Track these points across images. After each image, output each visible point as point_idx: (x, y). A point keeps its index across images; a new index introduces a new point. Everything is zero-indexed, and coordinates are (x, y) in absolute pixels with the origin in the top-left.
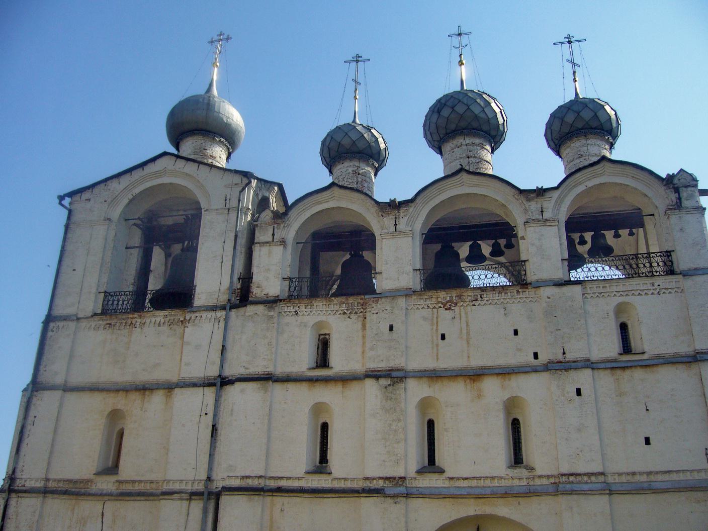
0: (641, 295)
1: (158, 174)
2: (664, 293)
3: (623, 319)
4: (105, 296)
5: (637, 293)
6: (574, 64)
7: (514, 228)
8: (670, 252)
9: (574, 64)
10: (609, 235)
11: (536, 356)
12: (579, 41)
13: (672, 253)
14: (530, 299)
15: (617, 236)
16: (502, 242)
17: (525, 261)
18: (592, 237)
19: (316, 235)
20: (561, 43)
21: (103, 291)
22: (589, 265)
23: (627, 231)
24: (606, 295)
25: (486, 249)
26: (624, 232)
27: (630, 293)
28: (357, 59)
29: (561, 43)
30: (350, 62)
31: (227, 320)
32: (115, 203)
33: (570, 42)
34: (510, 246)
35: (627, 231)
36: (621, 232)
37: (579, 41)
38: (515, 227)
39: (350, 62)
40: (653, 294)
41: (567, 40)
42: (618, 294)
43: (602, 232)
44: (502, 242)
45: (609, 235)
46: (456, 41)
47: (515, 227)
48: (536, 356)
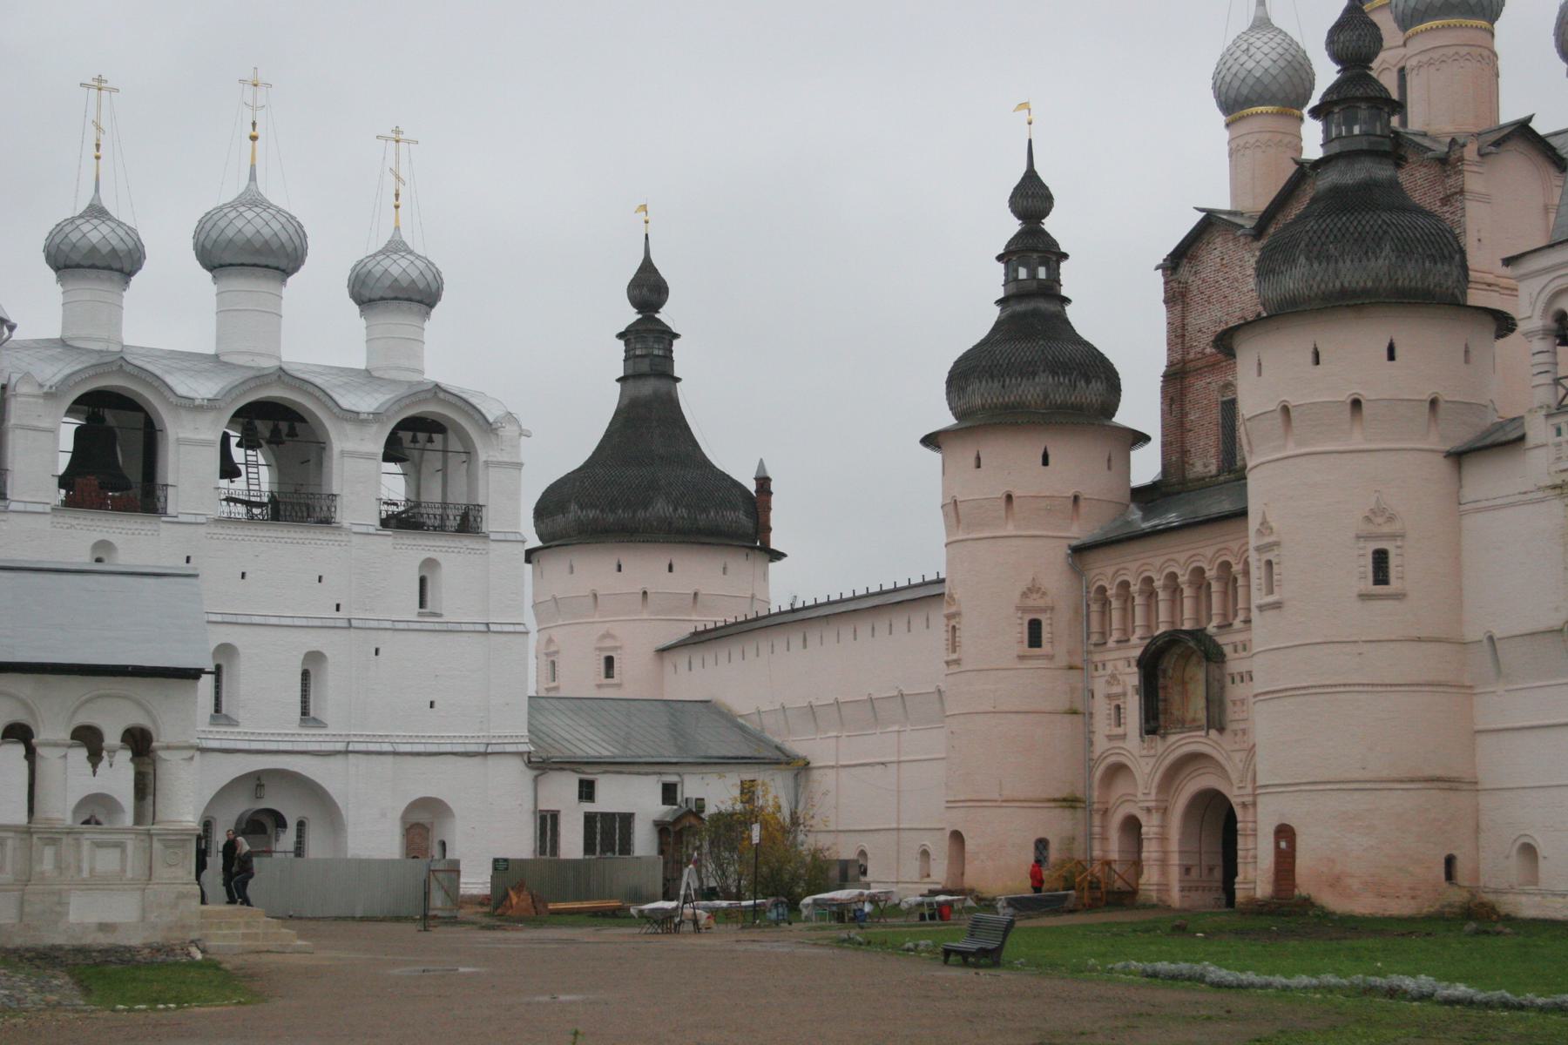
2: (470, 553)
3: (424, 574)
5: (444, 549)
6: (398, 177)
8: (481, 506)
9: (398, 177)
10: (406, 436)
11: (338, 607)
12: (409, 142)
13: (483, 508)
17: (335, 495)
20: (387, 139)
26: (421, 436)
28: (99, 84)
29: (387, 139)
30: (88, 86)
33: (397, 141)
34: (292, 433)
37: (409, 142)
39: (88, 86)
41: (394, 135)
44: (284, 426)
46: (249, 90)
48: (338, 607)
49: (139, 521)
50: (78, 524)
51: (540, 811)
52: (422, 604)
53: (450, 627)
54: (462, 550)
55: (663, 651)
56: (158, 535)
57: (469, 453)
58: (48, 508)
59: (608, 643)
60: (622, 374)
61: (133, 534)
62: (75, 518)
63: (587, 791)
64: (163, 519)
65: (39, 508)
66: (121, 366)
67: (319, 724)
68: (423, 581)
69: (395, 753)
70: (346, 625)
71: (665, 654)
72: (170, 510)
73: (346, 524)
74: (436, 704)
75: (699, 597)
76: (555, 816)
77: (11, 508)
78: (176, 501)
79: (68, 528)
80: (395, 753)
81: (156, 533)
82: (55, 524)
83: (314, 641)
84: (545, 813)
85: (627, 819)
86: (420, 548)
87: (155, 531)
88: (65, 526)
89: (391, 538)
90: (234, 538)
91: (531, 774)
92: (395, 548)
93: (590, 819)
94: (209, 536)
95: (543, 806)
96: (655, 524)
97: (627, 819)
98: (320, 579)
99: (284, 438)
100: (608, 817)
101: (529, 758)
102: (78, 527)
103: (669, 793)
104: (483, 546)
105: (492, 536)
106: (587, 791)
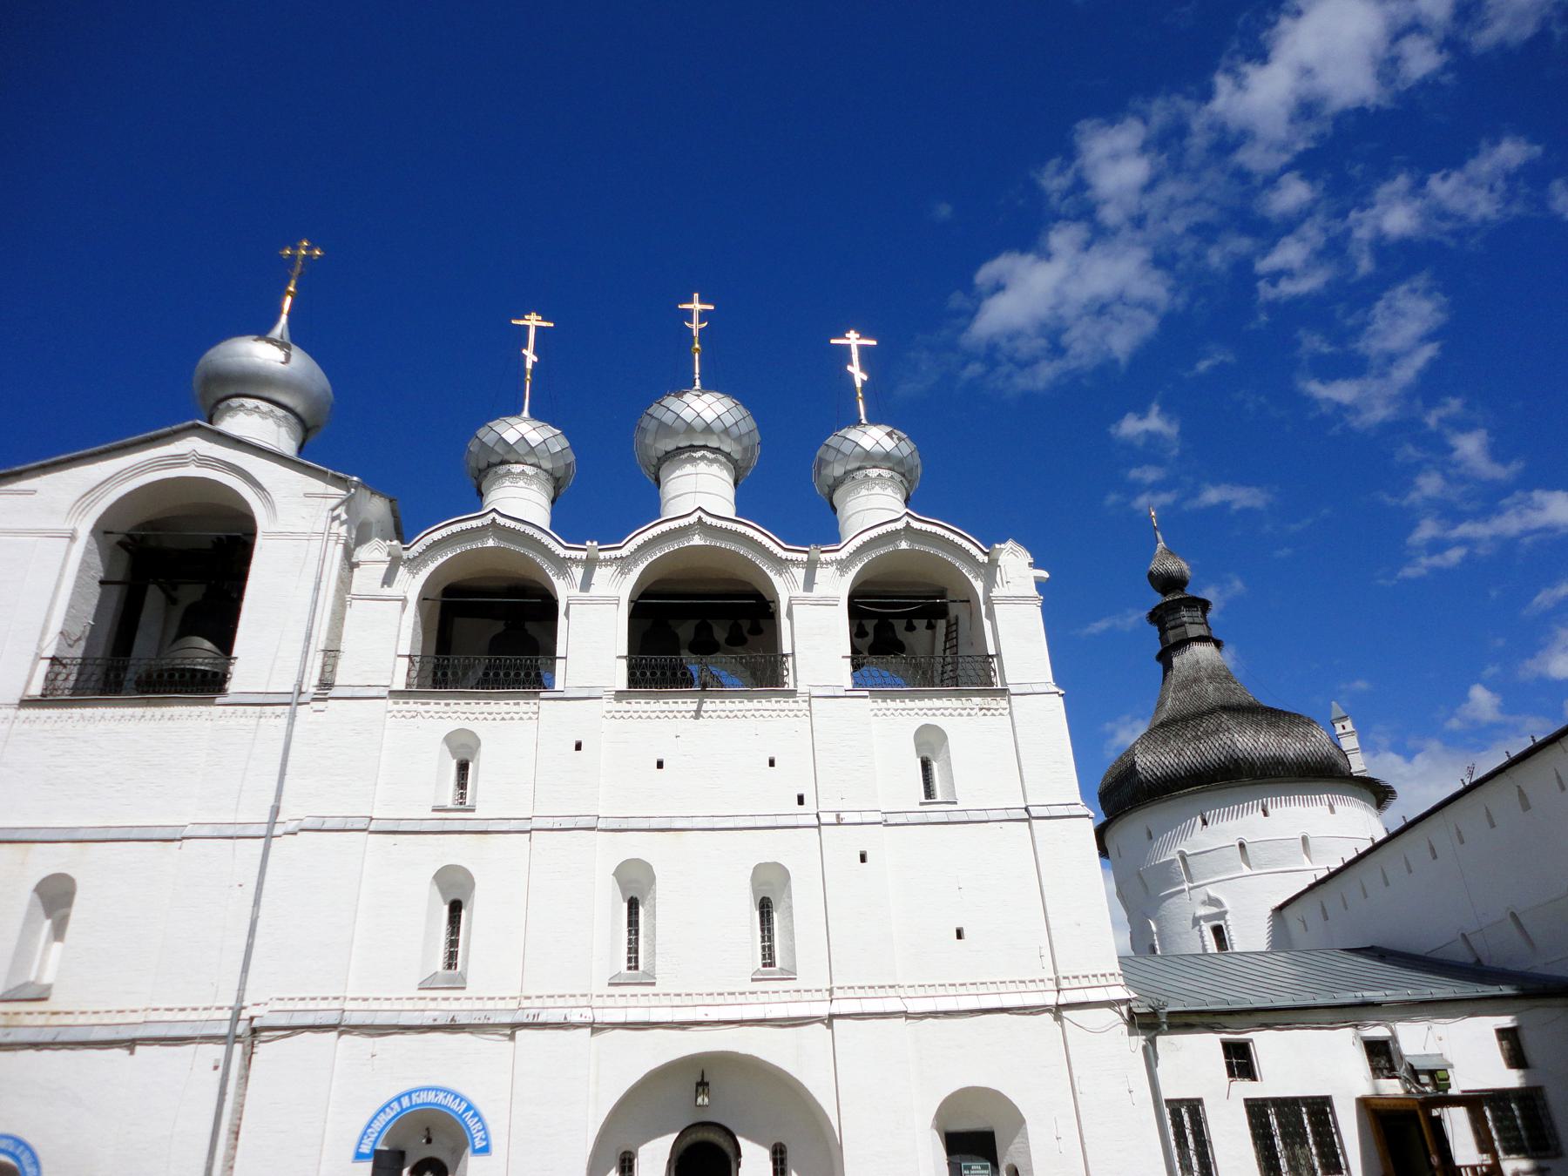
0: (953, 716)
1: (180, 460)
2: (985, 715)
4: (52, 665)
7: (771, 604)
11: (801, 800)
14: (795, 712)
15: (910, 628)
16: (746, 624)
18: (876, 628)
19: (449, 591)
21: (51, 656)
22: (873, 669)
23: (925, 622)
24: (904, 713)
25: (720, 633)
31: (293, 716)
32: (87, 502)
35: (925, 622)
36: (916, 622)
38: (773, 602)
40: (969, 715)
43: (890, 620)
44: (746, 624)
45: (900, 625)
47: (773, 602)
48: (801, 800)
49: (511, 702)
50: (428, 712)
51: (1167, 1101)
52: (929, 792)
54: (973, 712)
55: (1281, 908)
56: (538, 718)
57: (968, 601)
58: (385, 694)
59: (1214, 910)
60: (1159, 648)
61: (503, 719)
62: (423, 704)
63: (1240, 1061)
64: (542, 695)
66: (494, 520)
67: (789, 975)
69: (906, 1015)
70: (816, 823)
71: (1285, 912)
72: (559, 685)
74: (966, 933)
75: (1311, 841)
76: (1195, 1106)
78: (566, 674)
79: (413, 717)
80: (906, 1015)
83: (768, 848)
84: (1177, 1105)
85: (1320, 1108)
86: (912, 713)
87: (534, 713)
88: (408, 715)
89: (868, 700)
90: (646, 715)
91: (1140, 1040)
92: (876, 715)
93: (1256, 1109)
95: (1168, 1093)
96: (1231, 766)
97: (1320, 1108)
98: (772, 763)
99: (746, 634)
100: (1288, 1106)
101: (1130, 1010)
103: (1381, 1055)
104: (1004, 703)
105: (1013, 689)
106: (1240, 1061)
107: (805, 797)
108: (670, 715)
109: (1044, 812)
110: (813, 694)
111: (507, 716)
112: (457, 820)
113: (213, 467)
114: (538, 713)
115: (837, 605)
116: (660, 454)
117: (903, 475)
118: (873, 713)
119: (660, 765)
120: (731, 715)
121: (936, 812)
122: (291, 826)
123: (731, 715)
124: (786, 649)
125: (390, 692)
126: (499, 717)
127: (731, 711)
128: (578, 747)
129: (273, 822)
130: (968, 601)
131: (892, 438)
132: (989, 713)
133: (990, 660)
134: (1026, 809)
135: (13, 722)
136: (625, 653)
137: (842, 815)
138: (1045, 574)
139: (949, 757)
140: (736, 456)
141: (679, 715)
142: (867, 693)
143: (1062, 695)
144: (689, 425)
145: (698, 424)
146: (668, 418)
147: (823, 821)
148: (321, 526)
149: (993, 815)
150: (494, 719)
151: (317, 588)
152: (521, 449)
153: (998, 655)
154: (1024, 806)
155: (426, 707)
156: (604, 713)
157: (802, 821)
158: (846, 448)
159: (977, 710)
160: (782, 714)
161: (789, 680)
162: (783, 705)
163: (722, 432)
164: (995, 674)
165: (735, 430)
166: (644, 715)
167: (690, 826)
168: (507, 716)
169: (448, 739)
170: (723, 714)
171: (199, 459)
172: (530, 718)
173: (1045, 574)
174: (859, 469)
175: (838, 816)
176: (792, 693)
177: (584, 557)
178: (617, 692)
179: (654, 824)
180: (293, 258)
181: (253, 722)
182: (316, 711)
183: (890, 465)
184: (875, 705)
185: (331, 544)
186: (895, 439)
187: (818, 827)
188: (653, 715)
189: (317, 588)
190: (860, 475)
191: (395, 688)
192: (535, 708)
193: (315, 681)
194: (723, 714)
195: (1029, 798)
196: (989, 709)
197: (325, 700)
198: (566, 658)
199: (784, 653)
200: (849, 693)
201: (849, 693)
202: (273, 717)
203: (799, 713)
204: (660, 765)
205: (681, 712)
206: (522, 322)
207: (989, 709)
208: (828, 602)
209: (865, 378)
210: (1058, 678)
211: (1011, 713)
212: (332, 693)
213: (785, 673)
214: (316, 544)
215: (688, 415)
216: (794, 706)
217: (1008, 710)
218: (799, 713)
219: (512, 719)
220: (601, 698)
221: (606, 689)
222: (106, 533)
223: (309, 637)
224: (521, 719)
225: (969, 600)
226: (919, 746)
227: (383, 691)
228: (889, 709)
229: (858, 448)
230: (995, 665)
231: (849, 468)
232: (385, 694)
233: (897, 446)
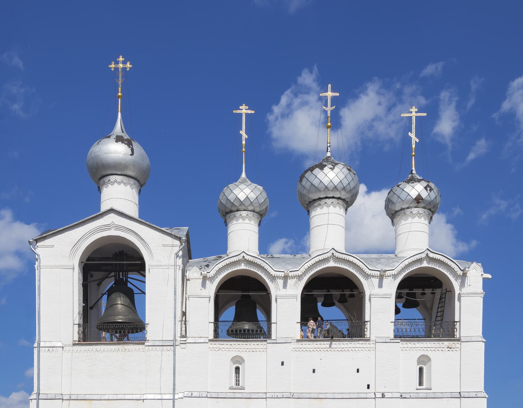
2: (449, 350)
5: (432, 349)
24: (414, 349)
27: (429, 349)
31: (174, 351)
38: (362, 293)
42: (421, 349)
47: (362, 293)
53: (437, 395)
54: (443, 349)
57: (451, 291)
64: (268, 341)
65: (202, 340)
68: (421, 370)
70: (374, 397)
73: (372, 338)
77: (188, 341)
81: (265, 350)
82: (211, 349)
88: (217, 349)
92: (402, 350)
94: (294, 350)
102: (223, 350)
107: (370, 385)
108: (318, 350)
109: (467, 395)
110: (377, 341)
111: (254, 350)
112: (238, 393)
113: (122, 230)
114: (267, 349)
115: (391, 298)
116: (310, 200)
117: (430, 210)
118: (401, 349)
119: (314, 371)
120: (343, 350)
121: (423, 393)
122: (181, 395)
123: (343, 350)
124: (367, 318)
125: (209, 340)
126: (251, 350)
127: (343, 348)
128: (283, 364)
129: (174, 394)
130: (451, 291)
131: (427, 190)
132: (450, 350)
133: (456, 323)
134: (460, 393)
135: (72, 352)
136: (300, 321)
137: (385, 394)
138: (489, 276)
139: (431, 369)
140: (347, 200)
141: (322, 350)
142: (399, 341)
143: (485, 342)
144: (326, 187)
145: (331, 186)
146: (316, 182)
147: (377, 396)
148: (172, 262)
149: (445, 395)
150: (249, 351)
151: (175, 294)
152: (247, 203)
153: (459, 322)
154: (459, 392)
155: (223, 346)
156: (292, 349)
157: (369, 396)
158: (403, 196)
159: (446, 348)
160: (363, 349)
161: (367, 334)
162: (365, 346)
163: (342, 190)
164: (457, 331)
165: (348, 188)
166: (308, 350)
167: (325, 397)
168: (254, 350)
169: (232, 359)
170: (339, 349)
171: (115, 227)
172: (263, 351)
173: (489, 276)
174: (408, 208)
175: (383, 394)
176: (368, 340)
177: (283, 276)
178: (297, 340)
179: (312, 396)
180: (116, 69)
181: (160, 353)
182: (182, 348)
183: (424, 205)
184: (402, 346)
185: (177, 270)
186: (428, 191)
187: (375, 398)
188: (311, 350)
189: (175, 294)
190: (408, 211)
191: (210, 339)
192: (265, 347)
193: (179, 335)
194: (339, 349)
195: (461, 389)
196: (451, 348)
197: (185, 344)
198: (276, 323)
199: (366, 320)
200: (392, 341)
201: (392, 341)
202: (167, 351)
203: (370, 349)
204: (314, 371)
205: (322, 348)
206: (238, 112)
207: (451, 348)
208: (386, 296)
209: (418, 141)
210: (485, 333)
211: (460, 349)
212: (189, 340)
213: (366, 330)
214: (172, 271)
215: (326, 181)
216: (369, 346)
217: (459, 349)
218: (370, 349)
219: (256, 351)
220: (291, 343)
221: (293, 338)
222: (82, 262)
223: (175, 317)
224: (260, 351)
225: (451, 290)
226: (419, 363)
227: (207, 340)
228: (408, 348)
229: (409, 197)
230: (457, 326)
231: (403, 207)
232: (208, 341)
233: (429, 194)
